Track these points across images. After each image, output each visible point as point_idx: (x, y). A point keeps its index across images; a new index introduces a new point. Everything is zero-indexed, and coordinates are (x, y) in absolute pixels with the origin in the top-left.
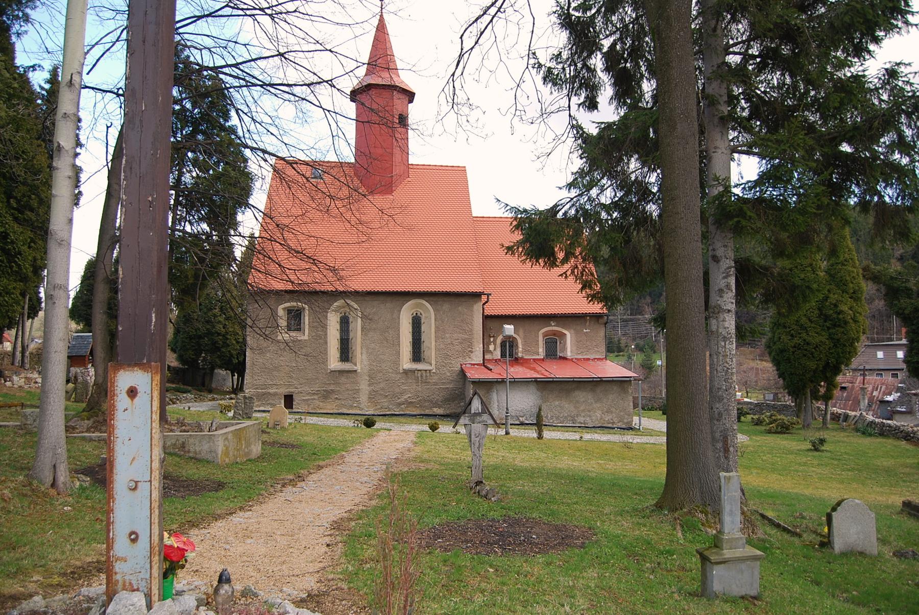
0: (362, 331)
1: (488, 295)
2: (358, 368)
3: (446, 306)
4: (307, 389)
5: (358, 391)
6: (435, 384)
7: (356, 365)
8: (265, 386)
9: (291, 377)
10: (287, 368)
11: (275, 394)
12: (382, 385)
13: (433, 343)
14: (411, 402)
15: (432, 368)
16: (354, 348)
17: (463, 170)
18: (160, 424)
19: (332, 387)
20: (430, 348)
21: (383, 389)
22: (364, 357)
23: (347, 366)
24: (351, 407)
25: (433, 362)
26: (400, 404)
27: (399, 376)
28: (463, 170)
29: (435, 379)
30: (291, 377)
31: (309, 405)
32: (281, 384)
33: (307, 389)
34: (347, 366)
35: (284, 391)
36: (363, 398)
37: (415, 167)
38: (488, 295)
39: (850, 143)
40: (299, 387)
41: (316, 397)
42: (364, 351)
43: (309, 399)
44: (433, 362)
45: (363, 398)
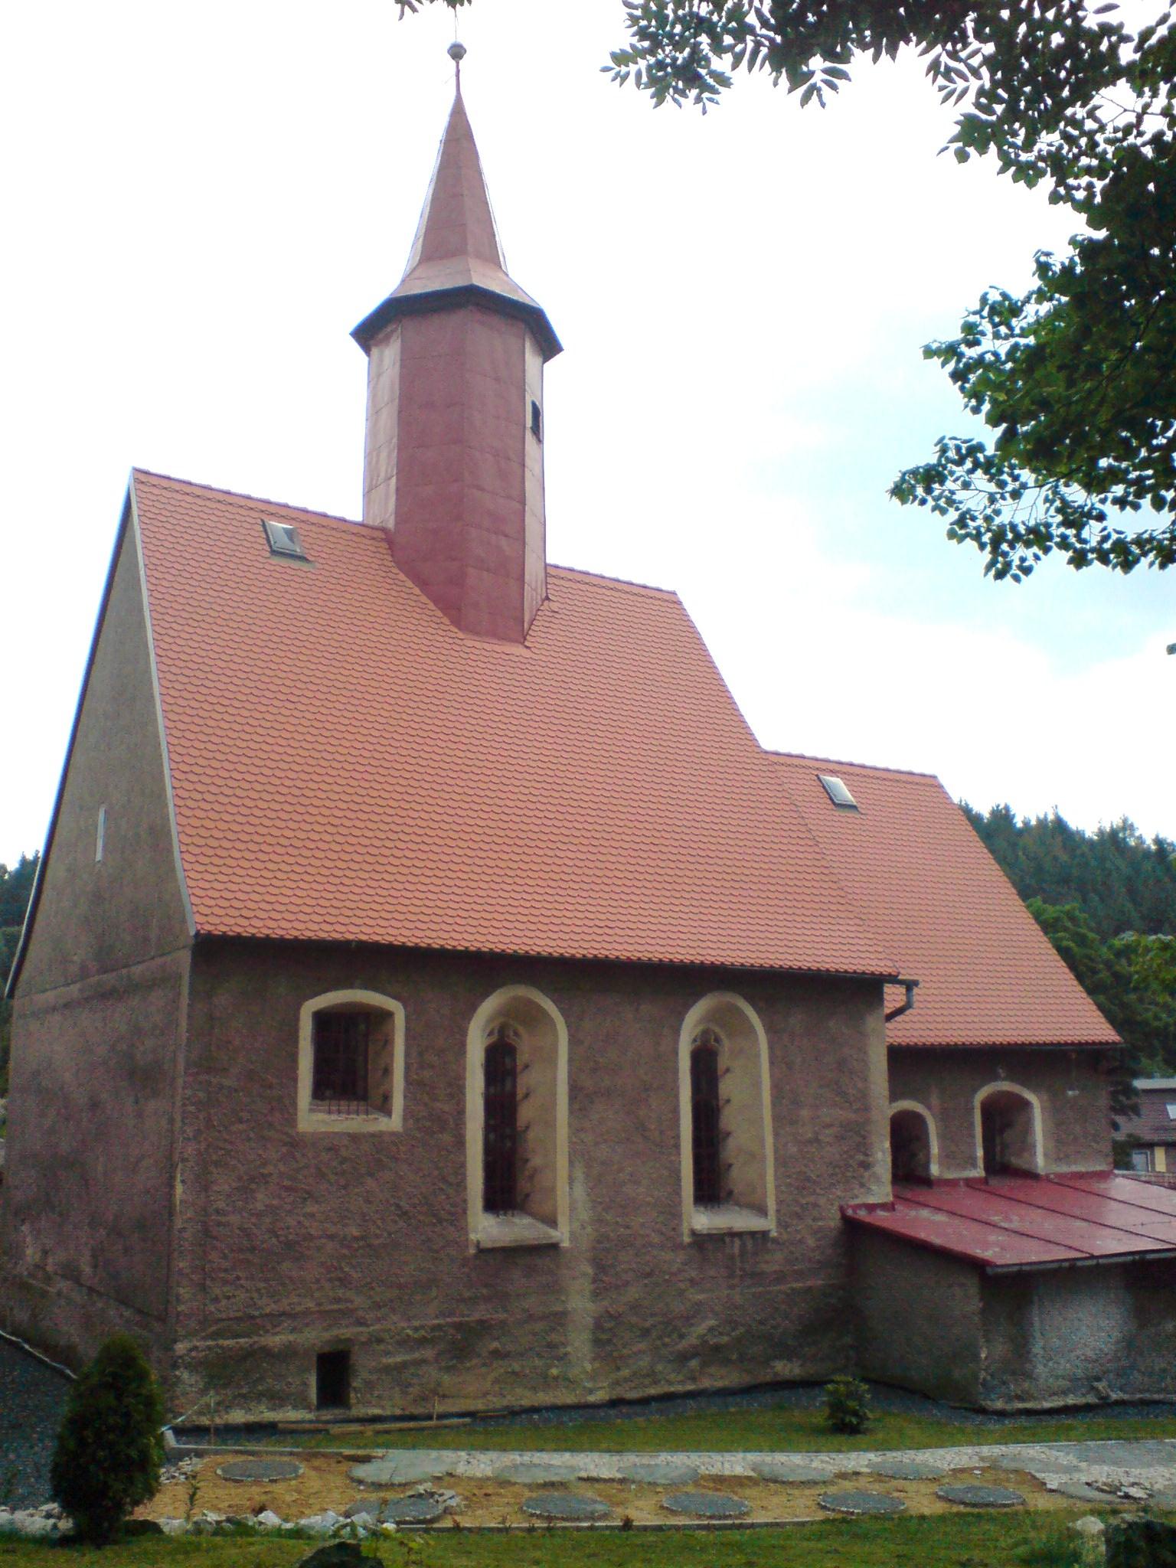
0: (573, 1097)
1: (910, 985)
2: (562, 1235)
3: (797, 1020)
4: (396, 1323)
5: (559, 1319)
6: (780, 1277)
7: (553, 1223)
8: (250, 1323)
9: (344, 1281)
10: (330, 1246)
11: (288, 1354)
12: (633, 1293)
13: (769, 1140)
14: (717, 1348)
15: (767, 1223)
16: (536, 1161)
17: (142, 478)
18: (556, 1209)
19: (480, 1312)
20: (755, 1157)
21: (635, 1307)
22: (580, 1191)
23: (516, 1229)
24: (547, 1382)
25: (771, 1204)
26: (683, 1358)
27: (681, 1257)
28: (142, 478)
29: (773, 1262)
30: (344, 1281)
31: (405, 1387)
32: (307, 1313)
33: (396, 1323)
34: (516, 1229)
35: (315, 1337)
36: (579, 1343)
37: (563, 574)
38: (910, 985)
39: (905, 11)
40: (370, 1316)
41: (428, 1353)
42: (579, 1174)
43: (404, 1365)
44: (771, 1204)
45: (579, 1343)
